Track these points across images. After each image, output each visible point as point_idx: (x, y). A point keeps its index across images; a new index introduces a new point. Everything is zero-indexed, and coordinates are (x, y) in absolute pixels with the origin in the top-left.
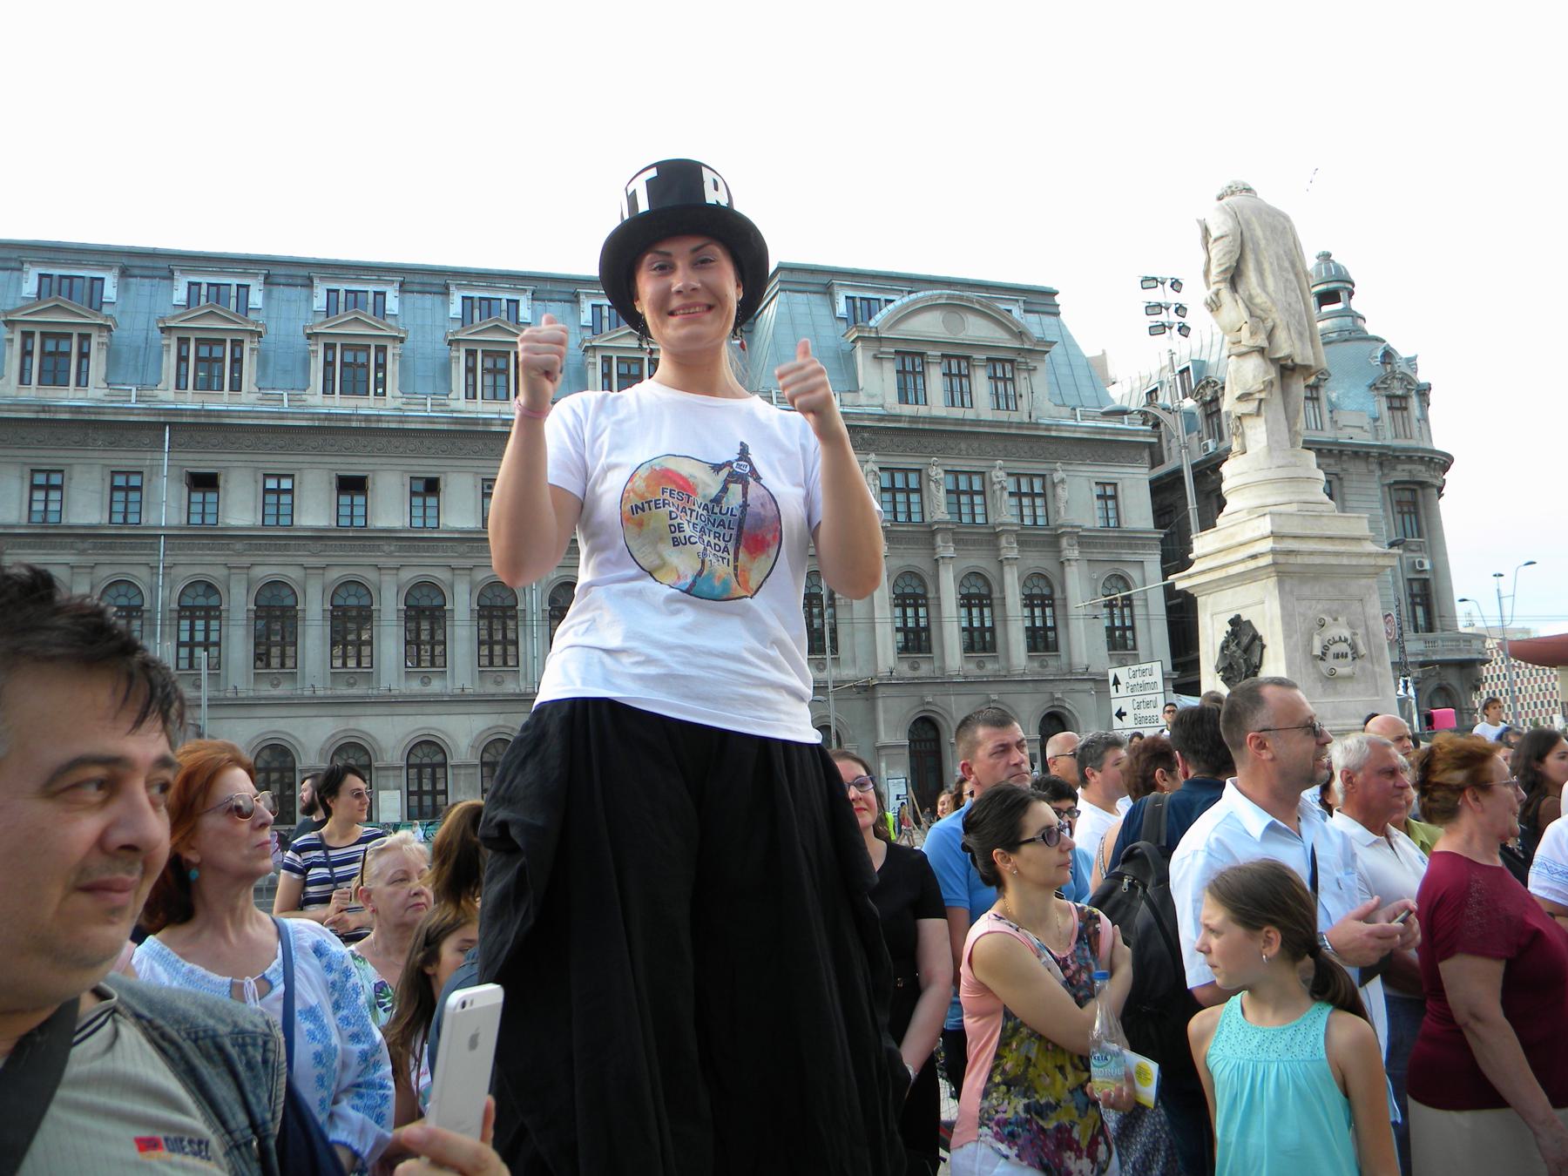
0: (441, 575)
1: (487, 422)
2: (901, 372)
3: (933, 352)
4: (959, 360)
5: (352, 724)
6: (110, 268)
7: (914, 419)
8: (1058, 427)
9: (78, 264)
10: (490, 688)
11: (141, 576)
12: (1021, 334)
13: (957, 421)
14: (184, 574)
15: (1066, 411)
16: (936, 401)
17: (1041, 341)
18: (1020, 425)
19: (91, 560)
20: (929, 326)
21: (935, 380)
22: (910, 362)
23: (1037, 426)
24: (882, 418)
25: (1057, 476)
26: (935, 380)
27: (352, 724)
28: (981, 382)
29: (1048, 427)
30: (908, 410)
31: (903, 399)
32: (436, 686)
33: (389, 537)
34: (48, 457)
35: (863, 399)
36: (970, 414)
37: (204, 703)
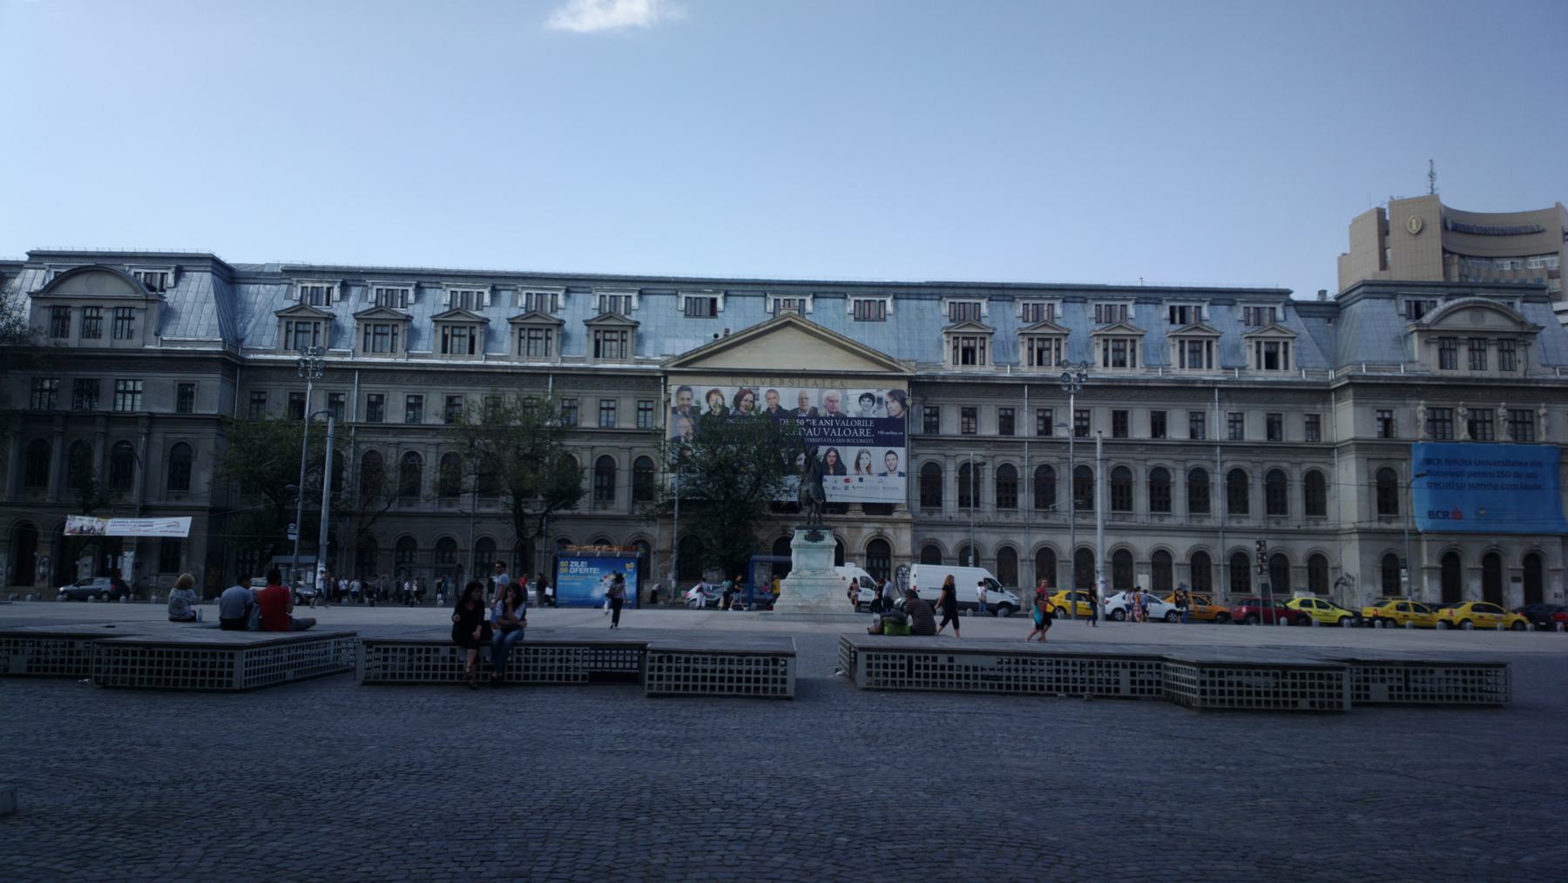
0: (1168, 464)
1: (1194, 381)
2: (1441, 351)
3: (1461, 337)
4: (1478, 341)
5: (1124, 539)
6: (982, 297)
7: (1449, 379)
8: (1544, 381)
9: (969, 297)
10: (1195, 523)
11: (1016, 462)
12: (1522, 323)
13: (1478, 380)
14: (1038, 461)
15: (1550, 370)
16: (1463, 367)
17: (1535, 326)
18: (1518, 381)
19: (992, 453)
20: (1461, 321)
21: (1463, 355)
22: (1446, 343)
23: (1530, 381)
24: (1430, 379)
25: (1542, 411)
26: (1463, 355)
27: (1124, 539)
28: (1492, 355)
29: (1538, 381)
30: (1447, 373)
31: (1442, 366)
32: (1168, 522)
33: (1141, 443)
34: (970, 402)
35: (1417, 367)
36: (1485, 374)
37: (1099, 530)
